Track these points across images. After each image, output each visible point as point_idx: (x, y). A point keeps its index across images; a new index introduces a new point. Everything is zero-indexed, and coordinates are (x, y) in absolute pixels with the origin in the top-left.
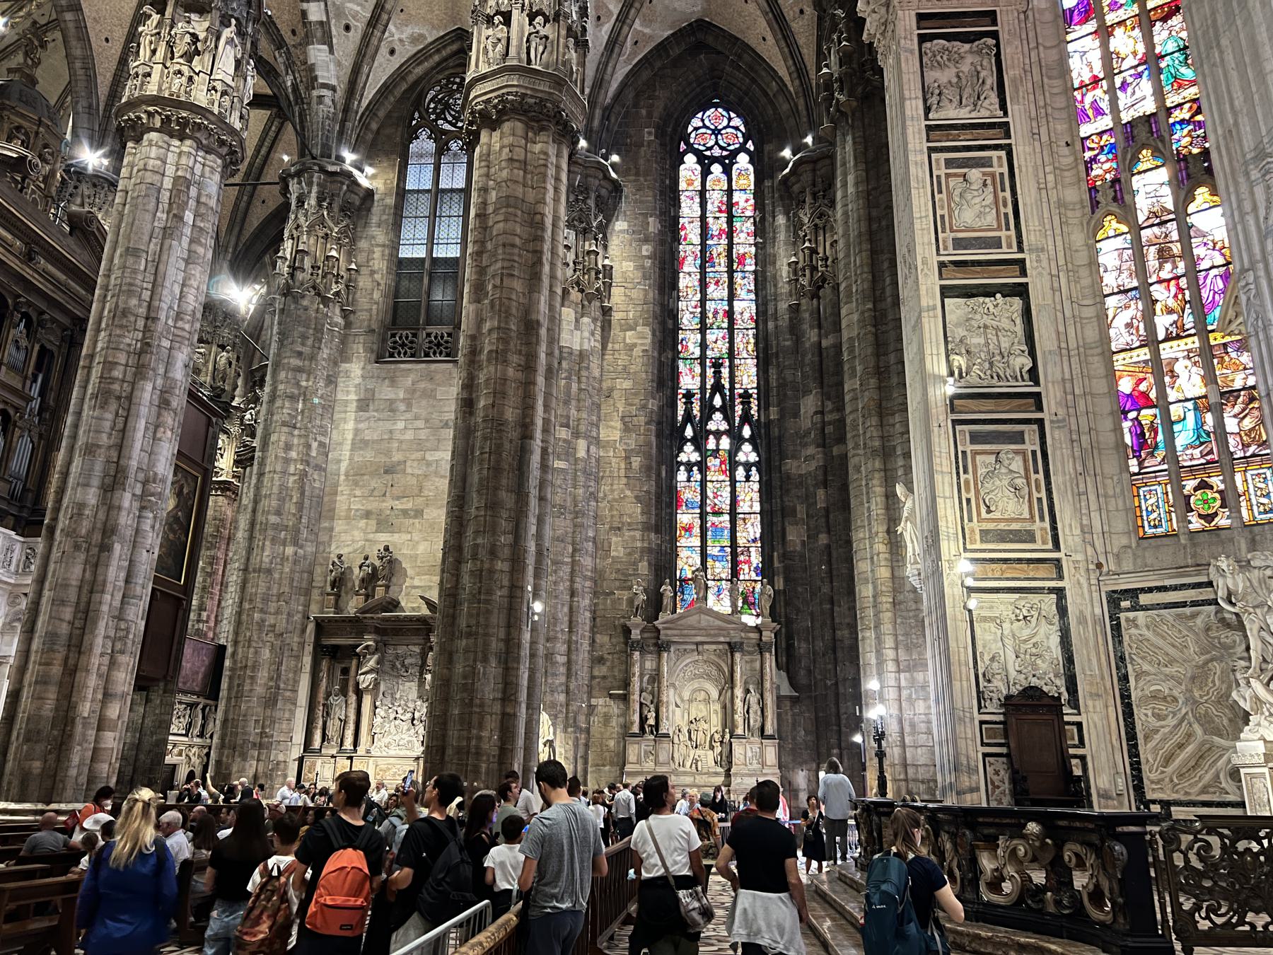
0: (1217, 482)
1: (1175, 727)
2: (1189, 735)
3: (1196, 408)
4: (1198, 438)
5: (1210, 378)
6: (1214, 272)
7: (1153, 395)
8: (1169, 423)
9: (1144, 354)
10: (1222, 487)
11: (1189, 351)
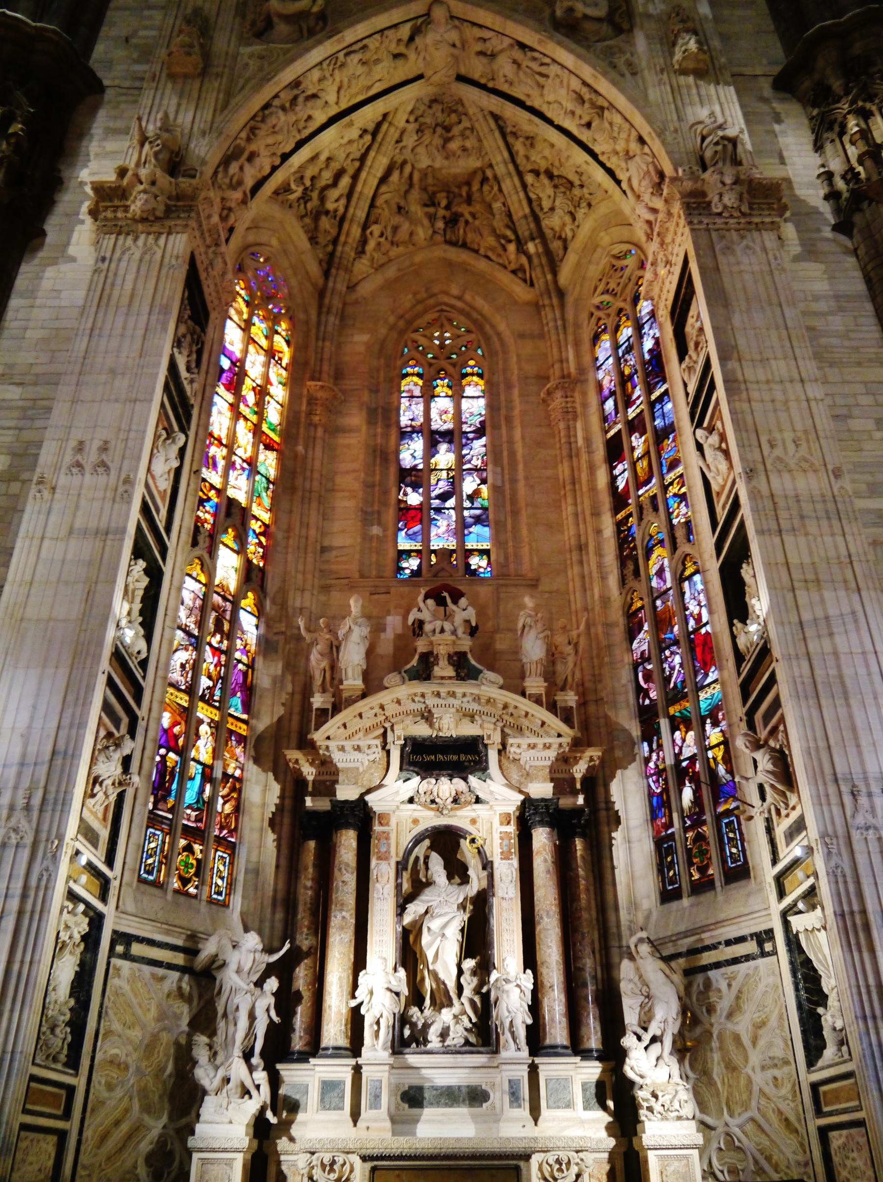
0: (197, 848)
1: (121, 1099)
2: (127, 1111)
4: (197, 802)
5: (216, 753)
6: (240, 666)
7: (181, 742)
8: (185, 777)
9: (183, 700)
10: (200, 856)
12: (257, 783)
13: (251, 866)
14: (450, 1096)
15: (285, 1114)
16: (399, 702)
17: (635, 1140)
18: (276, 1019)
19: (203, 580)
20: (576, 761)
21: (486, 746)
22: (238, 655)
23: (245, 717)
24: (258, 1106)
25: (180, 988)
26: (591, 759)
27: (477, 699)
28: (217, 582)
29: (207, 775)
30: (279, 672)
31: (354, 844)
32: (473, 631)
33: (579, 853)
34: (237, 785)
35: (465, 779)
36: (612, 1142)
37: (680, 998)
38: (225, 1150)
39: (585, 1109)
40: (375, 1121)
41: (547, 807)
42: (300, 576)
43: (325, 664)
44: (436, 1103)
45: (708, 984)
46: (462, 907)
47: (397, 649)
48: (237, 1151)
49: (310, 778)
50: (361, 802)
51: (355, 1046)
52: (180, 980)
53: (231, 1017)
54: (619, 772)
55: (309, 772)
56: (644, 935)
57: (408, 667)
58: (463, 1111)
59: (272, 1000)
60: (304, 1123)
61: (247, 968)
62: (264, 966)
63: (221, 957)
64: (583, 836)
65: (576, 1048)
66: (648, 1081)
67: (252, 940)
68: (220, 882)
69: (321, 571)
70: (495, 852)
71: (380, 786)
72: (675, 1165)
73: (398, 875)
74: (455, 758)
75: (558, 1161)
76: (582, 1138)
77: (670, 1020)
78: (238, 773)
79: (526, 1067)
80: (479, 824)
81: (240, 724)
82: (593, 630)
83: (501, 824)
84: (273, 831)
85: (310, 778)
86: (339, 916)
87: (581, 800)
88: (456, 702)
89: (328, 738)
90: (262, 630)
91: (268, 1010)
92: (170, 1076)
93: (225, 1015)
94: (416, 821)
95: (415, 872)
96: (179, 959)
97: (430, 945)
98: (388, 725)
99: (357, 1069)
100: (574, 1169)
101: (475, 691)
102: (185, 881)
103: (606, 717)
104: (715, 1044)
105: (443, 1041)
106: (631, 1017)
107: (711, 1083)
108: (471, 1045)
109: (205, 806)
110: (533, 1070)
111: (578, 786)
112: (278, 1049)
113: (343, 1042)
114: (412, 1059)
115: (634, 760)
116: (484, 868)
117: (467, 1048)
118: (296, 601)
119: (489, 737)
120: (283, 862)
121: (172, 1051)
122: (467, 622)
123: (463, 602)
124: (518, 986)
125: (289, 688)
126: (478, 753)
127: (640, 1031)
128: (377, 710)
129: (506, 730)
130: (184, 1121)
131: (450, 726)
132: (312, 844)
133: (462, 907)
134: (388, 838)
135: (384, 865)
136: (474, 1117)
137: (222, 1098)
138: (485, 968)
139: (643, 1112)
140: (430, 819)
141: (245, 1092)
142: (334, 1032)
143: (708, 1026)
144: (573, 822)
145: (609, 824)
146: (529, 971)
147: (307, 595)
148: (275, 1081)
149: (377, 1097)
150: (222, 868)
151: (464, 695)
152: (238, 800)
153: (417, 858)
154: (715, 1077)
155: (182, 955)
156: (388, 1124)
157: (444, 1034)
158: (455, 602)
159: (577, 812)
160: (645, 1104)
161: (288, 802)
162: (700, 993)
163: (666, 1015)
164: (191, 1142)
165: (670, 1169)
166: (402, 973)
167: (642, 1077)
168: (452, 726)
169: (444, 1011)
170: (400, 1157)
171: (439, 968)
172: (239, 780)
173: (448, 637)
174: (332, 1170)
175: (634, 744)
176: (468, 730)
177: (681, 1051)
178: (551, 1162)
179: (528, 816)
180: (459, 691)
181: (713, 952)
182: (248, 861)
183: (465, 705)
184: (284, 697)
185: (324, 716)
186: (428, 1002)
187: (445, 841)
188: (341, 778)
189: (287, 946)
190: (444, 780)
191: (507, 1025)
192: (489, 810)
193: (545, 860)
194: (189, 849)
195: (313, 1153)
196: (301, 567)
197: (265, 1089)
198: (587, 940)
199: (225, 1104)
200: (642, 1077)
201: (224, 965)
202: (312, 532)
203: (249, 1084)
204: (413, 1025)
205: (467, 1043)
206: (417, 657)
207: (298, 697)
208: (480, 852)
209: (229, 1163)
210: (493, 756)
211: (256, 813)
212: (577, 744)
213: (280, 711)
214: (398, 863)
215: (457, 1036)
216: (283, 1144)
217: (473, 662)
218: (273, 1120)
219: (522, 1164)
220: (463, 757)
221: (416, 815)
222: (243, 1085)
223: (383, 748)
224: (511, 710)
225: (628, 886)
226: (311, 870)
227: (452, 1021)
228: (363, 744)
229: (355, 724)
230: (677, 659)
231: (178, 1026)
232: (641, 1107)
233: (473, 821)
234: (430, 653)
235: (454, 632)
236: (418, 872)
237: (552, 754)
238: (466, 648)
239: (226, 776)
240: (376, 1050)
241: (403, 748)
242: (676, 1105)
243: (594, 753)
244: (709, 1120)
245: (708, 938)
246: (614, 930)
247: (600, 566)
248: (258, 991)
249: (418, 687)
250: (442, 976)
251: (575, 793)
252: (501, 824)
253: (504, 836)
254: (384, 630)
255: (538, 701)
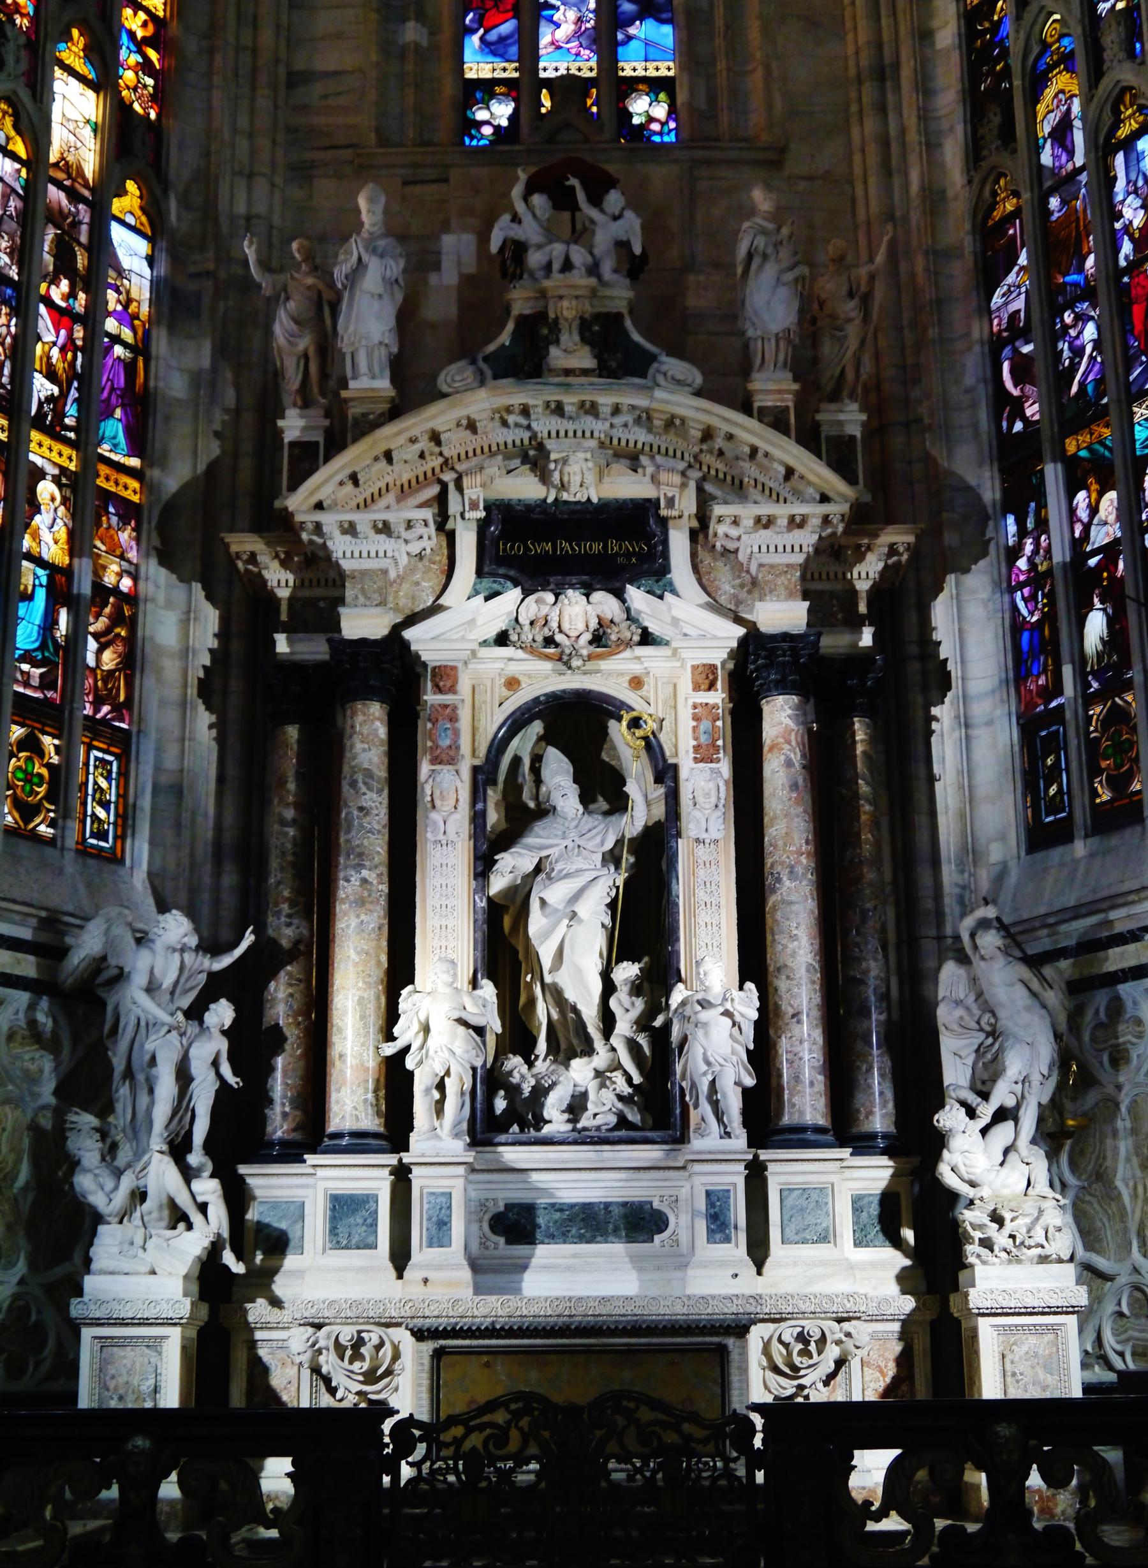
0: (49, 742)
3: (50, 588)
4: (43, 647)
5: (77, 543)
6: (118, 350)
10: (55, 760)
11: (63, 470)
12: (169, 604)
13: (164, 779)
14: (589, 1222)
15: (259, 1258)
16: (472, 426)
17: (954, 1299)
18: (232, 1080)
19: (23, 154)
20: (861, 558)
21: (664, 522)
22: (111, 325)
23: (134, 462)
24: (206, 1243)
25: (32, 1023)
26: (892, 550)
27: (644, 418)
28: (53, 158)
29: (60, 588)
30: (206, 363)
31: (382, 731)
32: (634, 267)
33: (860, 749)
34: (126, 610)
35: (619, 594)
36: (908, 1304)
37: (1057, 1036)
38: (145, 1322)
39: (857, 1244)
40: (440, 1267)
41: (795, 652)
42: (243, 144)
43: (305, 342)
44: (561, 1234)
45: (1116, 1008)
46: (612, 858)
47: (465, 307)
48: (169, 1322)
49: (284, 593)
50: (395, 641)
51: (396, 1127)
52: (32, 1007)
53: (141, 1077)
54: (951, 579)
55: (280, 580)
56: (990, 912)
57: (492, 348)
58: (617, 1249)
59: (223, 1045)
60: (300, 1273)
61: (168, 982)
62: (203, 978)
63: (112, 961)
64: (868, 712)
65: (844, 1130)
66: (985, 1192)
67: (176, 928)
68: (101, 813)
69: (291, 130)
70: (681, 745)
71: (435, 609)
72: (1032, 1342)
73: (477, 793)
74: (597, 547)
75: (802, 1338)
76: (849, 1296)
77: (1036, 1078)
78: (126, 584)
79: (741, 1168)
80: (648, 690)
81: (124, 479)
82: (903, 267)
83: (697, 688)
84: (209, 708)
85: (284, 593)
86: (355, 879)
87: (867, 638)
88: (599, 427)
89: (319, 506)
90: (162, 269)
91: (215, 1064)
92: (26, 1188)
93: (129, 1074)
94: (512, 684)
95: (513, 788)
96: (27, 966)
97: (547, 934)
98: (448, 477)
99: (402, 1175)
100: (833, 1352)
101: (642, 402)
102: (27, 811)
103: (928, 459)
104: (1123, 1123)
105: (574, 1120)
106: (956, 1073)
107: (1112, 1195)
108: (631, 1126)
109: (59, 656)
110: (756, 1175)
111: (863, 608)
112: (238, 1138)
113: (370, 1122)
114: (512, 1155)
115: (985, 554)
116: (658, 780)
117: (622, 1133)
118: (237, 199)
119: (671, 502)
120: (232, 771)
121: (26, 1142)
122: (623, 246)
123: (614, 199)
124: (727, 1013)
125: (230, 397)
126: (648, 537)
127: (972, 1099)
128: (424, 444)
129: (709, 487)
130: (60, 1271)
131: (586, 480)
132: (292, 732)
133: (612, 858)
134: (454, 719)
135: (446, 774)
136: (637, 1261)
137: (132, 1229)
138: (659, 978)
139: (972, 1250)
140: (542, 678)
141: (178, 1218)
142: (351, 1103)
143: (1110, 1089)
144: (849, 684)
145: (925, 689)
146: (750, 986)
147: (261, 187)
148: (237, 1197)
149: (443, 1223)
150: (104, 784)
151: (616, 410)
152: (131, 642)
153: (517, 761)
154: (1119, 1183)
155: (32, 958)
156: (466, 1274)
157: (576, 1106)
158: (596, 201)
159: (859, 660)
160: (977, 1235)
161: (235, 645)
162: (1100, 1026)
163: (1028, 1069)
164: (76, 1309)
165: (1020, 1351)
166: (488, 990)
167: (973, 1184)
168: (590, 478)
169: (576, 1063)
170: (491, 1332)
171: (562, 978)
172: (131, 599)
173: (579, 279)
174: (357, 1356)
175: (987, 518)
176: (627, 486)
177: (1053, 1135)
178: (787, 1338)
179: (755, 669)
180: (606, 401)
181: (1131, 947)
182: (158, 768)
183: (617, 433)
184: (219, 418)
185: (307, 459)
186: (542, 1046)
187: (577, 724)
188: (349, 594)
189: (249, 939)
190: (574, 597)
191: (704, 1087)
192: (669, 658)
193: (789, 763)
194: (30, 744)
195: (319, 1327)
196: (243, 122)
197: (218, 1213)
198: (872, 924)
199: (139, 1240)
200: (973, 1184)
201: (121, 977)
202: (267, 37)
203: (184, 1201)
204: (513, 1091)
205: (623, 1122)
206: (510, 326)
207: (248, 418)
208: (652, 747)
209: (154, 1345)
210: (679, 543)
211: (171, 669)
212: (864, 520)
213: (214, 449)
214: (475, 770)
215: (602, 1108)
216: (258, 1310)
217: (636, 337)
218: (238, 1268)
219: (730, 1342)
220: (613, 546)
221: (513, 669)
222: (172, 1205)
223: (441, 527)
224: (719, 442)
225: (962, 816)
226: (292, 786)
227: (592, 1081)
228: (396, 517)
229: (377, 476)
230: (1090, 332)
231: (35, 1096)
232: (969, 1239)
233: (636, 683)
234: (540, 317)
235: (593, 270)
236: (519, 789)
237: (807, 539)
238: (621, 306)
239: (101, 592)
240: (437, 1138)
241: (482, 527)
242: (1039, 1235)
243: (899, 537)
244: (1102, 1263)
245: (1121, 919)
246: (929, 904)
247: (925, 115)
248: (192, 1028)
249: (515, 395)
250: (570, 995)
251: (855, 623)
252: (697, 688)
253: (701, 713)
254: (437, 267)
255: (777, 421)
